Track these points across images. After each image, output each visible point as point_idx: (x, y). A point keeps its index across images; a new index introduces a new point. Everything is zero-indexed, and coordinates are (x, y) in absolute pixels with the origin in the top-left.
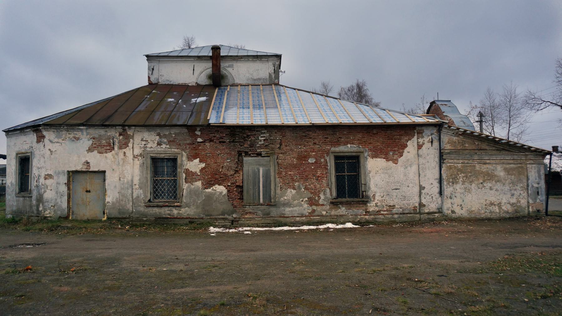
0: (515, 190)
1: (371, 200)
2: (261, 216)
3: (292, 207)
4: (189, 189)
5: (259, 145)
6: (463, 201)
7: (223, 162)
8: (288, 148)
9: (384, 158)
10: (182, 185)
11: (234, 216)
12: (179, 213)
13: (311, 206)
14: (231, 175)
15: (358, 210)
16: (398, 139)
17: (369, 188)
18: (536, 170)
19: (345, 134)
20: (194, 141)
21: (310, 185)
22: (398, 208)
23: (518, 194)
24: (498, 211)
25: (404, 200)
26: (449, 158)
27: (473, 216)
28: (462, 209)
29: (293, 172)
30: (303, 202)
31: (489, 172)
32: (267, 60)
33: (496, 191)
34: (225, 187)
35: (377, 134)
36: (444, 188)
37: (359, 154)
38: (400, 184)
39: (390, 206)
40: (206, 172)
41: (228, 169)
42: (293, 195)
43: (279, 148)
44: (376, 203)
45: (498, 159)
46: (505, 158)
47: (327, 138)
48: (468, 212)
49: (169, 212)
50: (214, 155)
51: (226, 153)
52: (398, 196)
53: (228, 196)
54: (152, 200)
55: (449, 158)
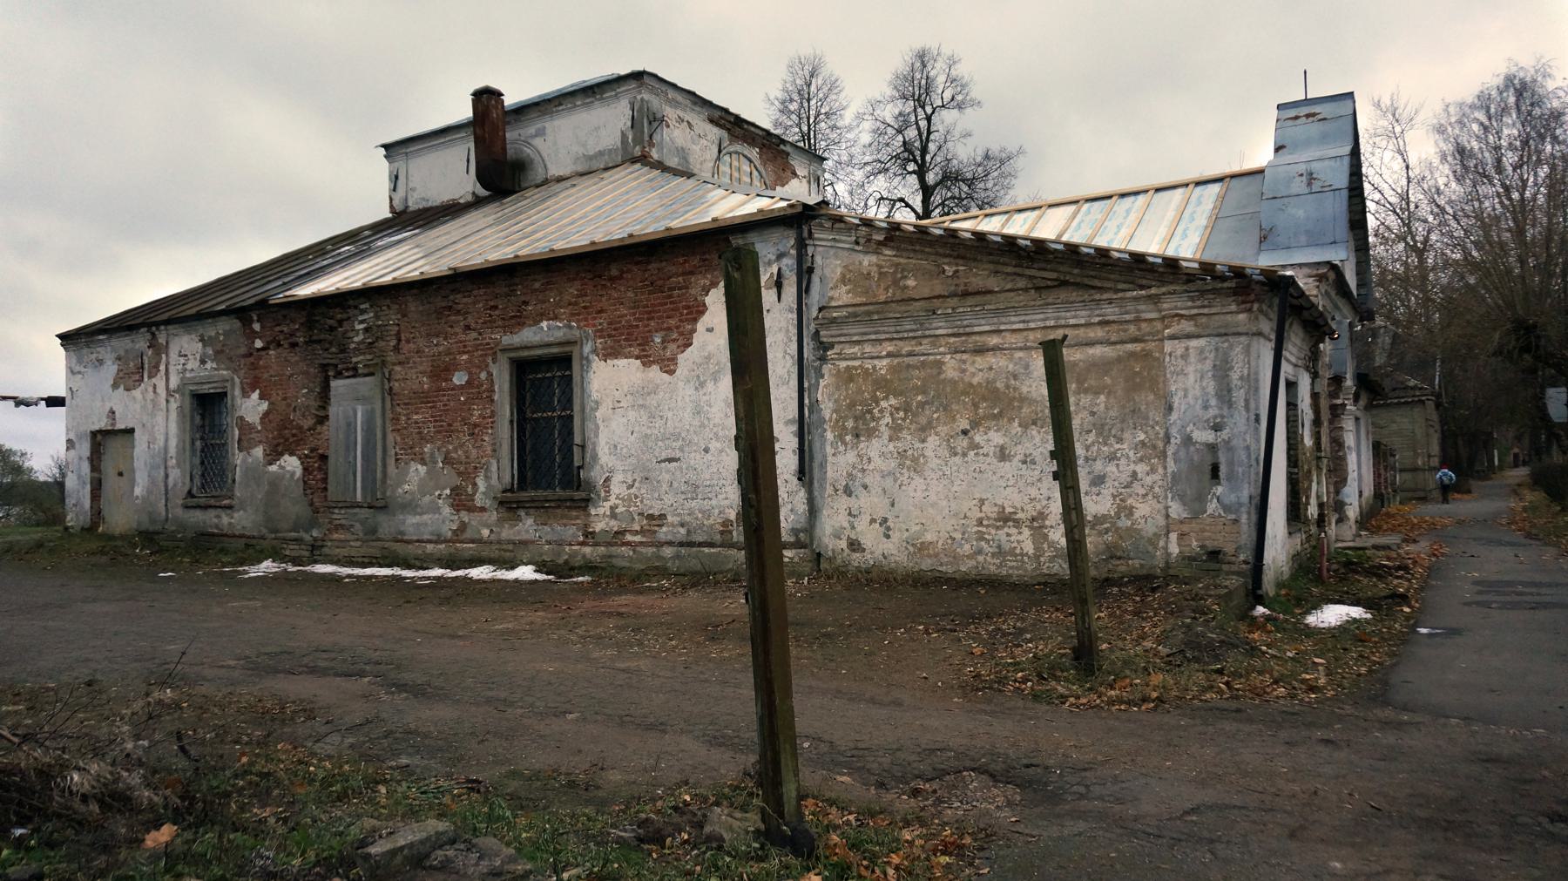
0: (1112, 457)
1: (599, 496)
2: (361, 535)
6: (893, 505)
8: (412, 345)
9: (637, 358)
10: (233, 455)
11: (315, 533)
12: (230, 524)
13: (458, 511)
14: (309, 430)
15: (565, 525)
16: (680, 289)
17: (595, 457)
18: (1208, 364)
19: (536, 290)
21: (456, 450)
22: (673, 525)
23: (1125, 478)
24: (1029, 547)
25: (693, 499)
26: (842, 339)
27: (926, 564)
28: (888, 537)
29: (423, 413)
30: (441, 501)
31: (999, 385)
32: (616, 95)
33: (1024, 462)
34: (300, 459)
35: (620, 277)
36: (825, 456)
37: (567, 349)
38: (680, 443)
39: (651, 517)
40: (270, 422)
43: (397, 349)
44: (611, 508)
45: (1032, 325)
46: (1063, 322)
47: (496, 307)
48: (911, 549)
49: (216, 520)
52: (675, 485)
53: (305, 482)
54: (194, 491)
55: (842, 339)
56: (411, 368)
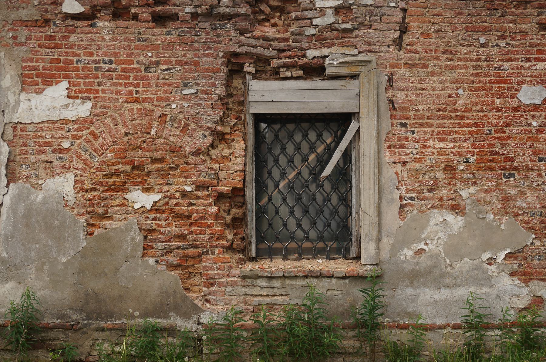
3: (447, 287)
4: (22, 207)
5: (312, 31)
7: (166, 99)
13: (526, 282)
14: (197, 153)
20: (47, 11)
41: (186, 125)
42: (451, 236)
43: (398, 43)
50: (131, 71)
51: (178, 62)
56: (433, 74)
